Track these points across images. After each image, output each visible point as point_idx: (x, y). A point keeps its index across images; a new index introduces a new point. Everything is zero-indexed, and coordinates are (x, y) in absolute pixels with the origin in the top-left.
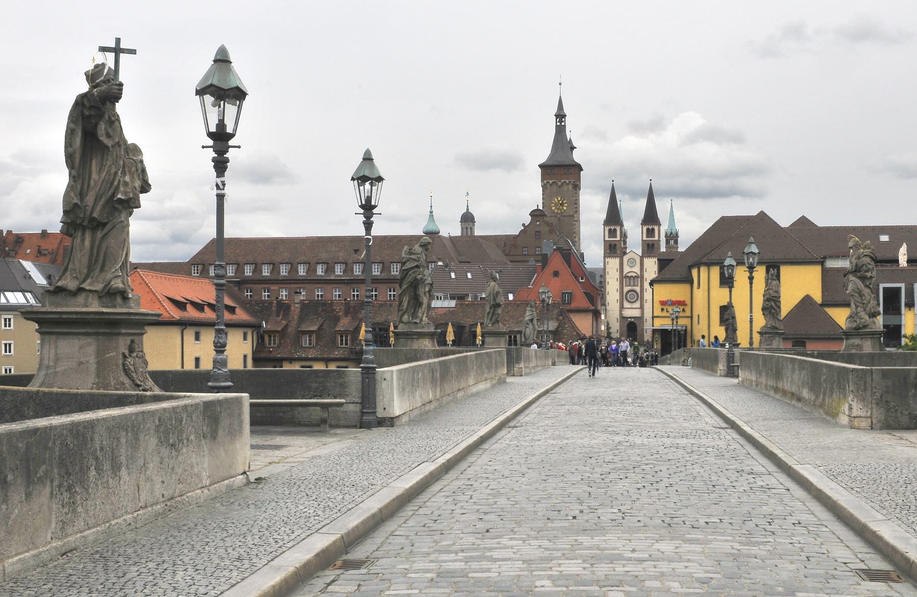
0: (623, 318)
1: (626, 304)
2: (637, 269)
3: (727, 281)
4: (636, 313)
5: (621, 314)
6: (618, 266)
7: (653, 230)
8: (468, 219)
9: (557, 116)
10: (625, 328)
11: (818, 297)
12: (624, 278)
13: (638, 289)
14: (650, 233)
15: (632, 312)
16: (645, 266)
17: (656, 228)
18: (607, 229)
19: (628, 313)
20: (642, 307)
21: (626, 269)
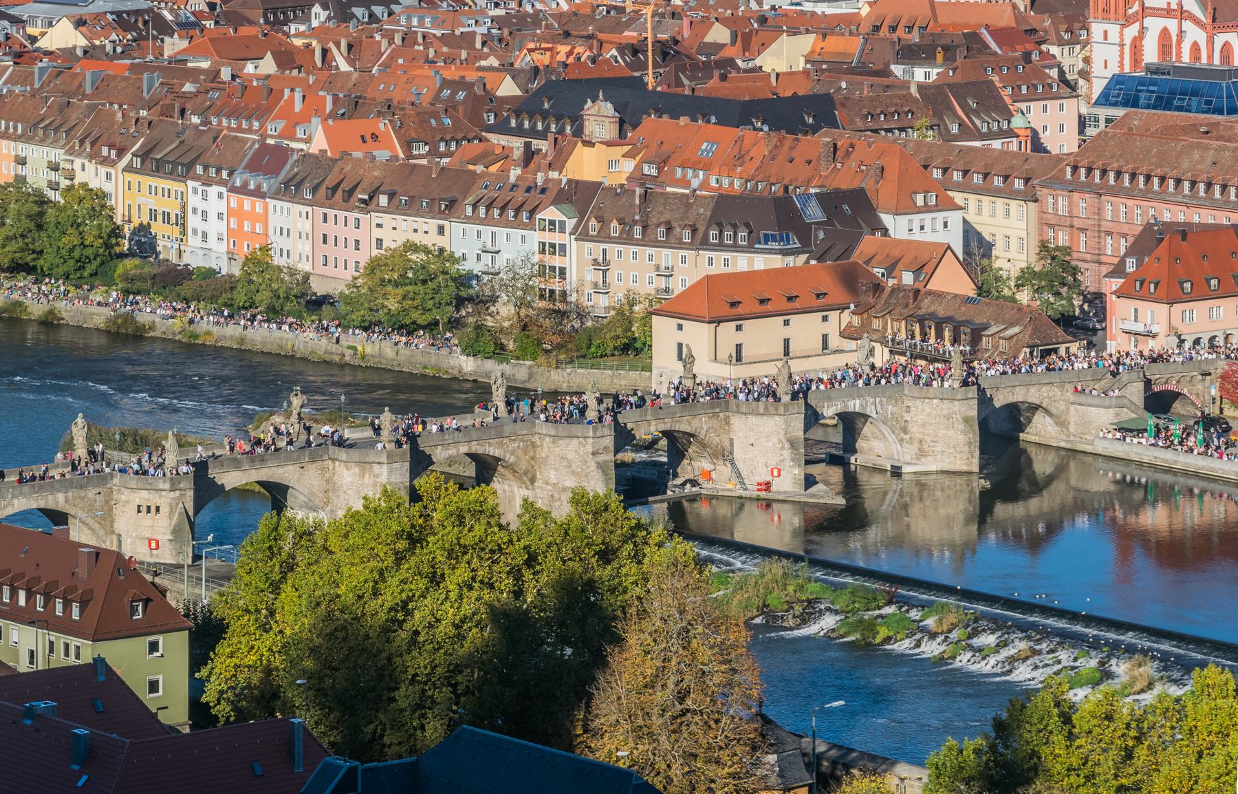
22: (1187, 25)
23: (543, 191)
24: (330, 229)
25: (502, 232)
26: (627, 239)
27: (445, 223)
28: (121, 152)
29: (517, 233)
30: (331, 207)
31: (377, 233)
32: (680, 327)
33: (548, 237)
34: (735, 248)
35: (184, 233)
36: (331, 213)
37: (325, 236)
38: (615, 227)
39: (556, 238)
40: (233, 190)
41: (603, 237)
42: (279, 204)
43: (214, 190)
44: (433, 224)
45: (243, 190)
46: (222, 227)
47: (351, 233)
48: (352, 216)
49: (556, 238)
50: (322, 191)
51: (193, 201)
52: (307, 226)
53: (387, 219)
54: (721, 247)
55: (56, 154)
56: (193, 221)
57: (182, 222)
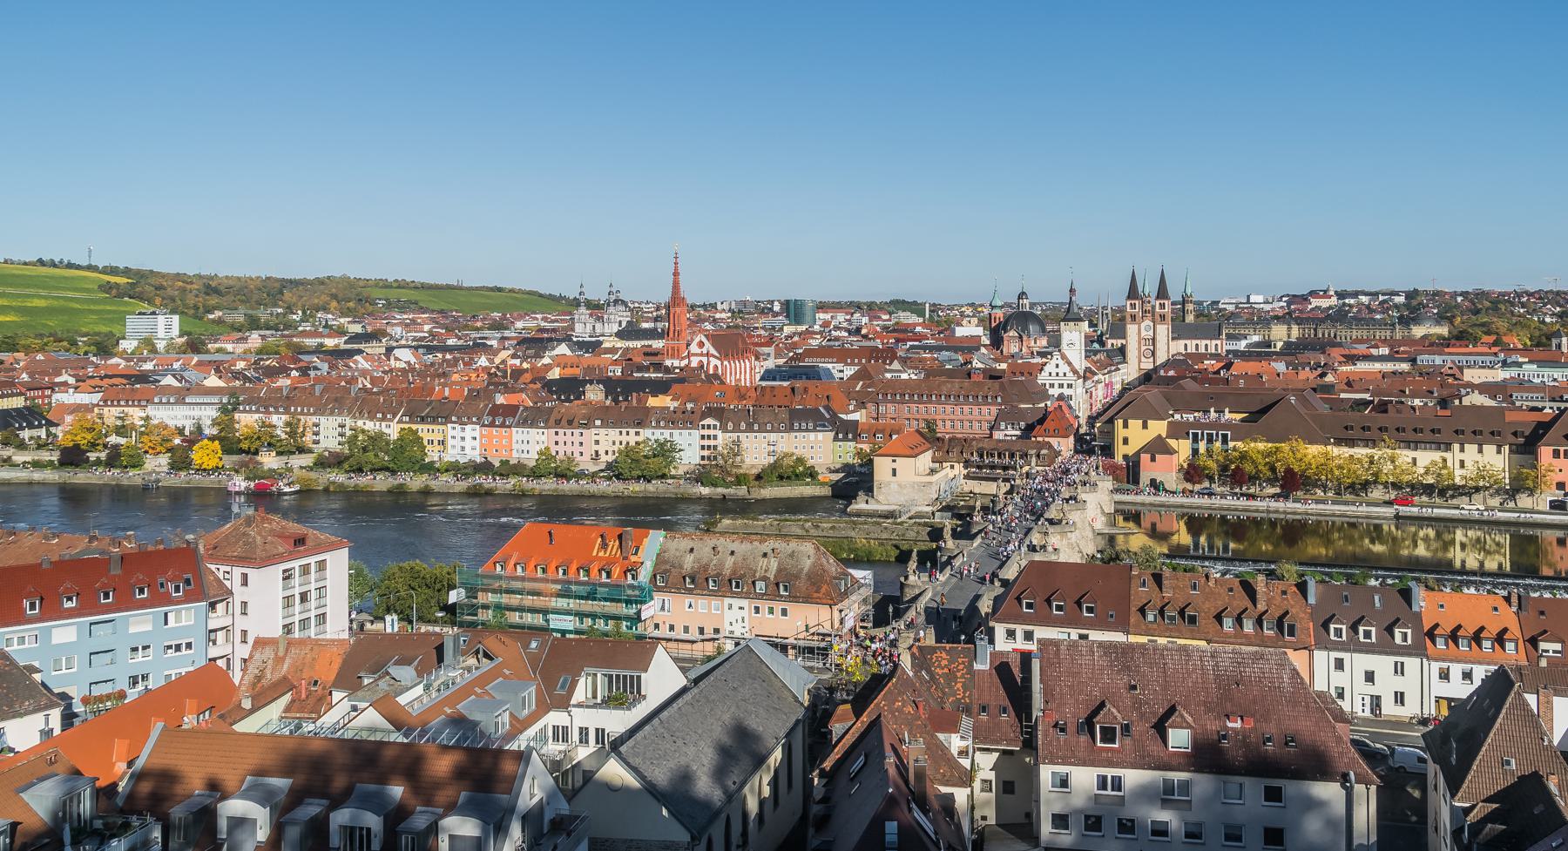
1: (1143, 359)
2: (1151, 333)
3: (1126, 426)
9: (1071, 291)
14: (1162, 306)
16: (1158, 331)
18: (1129, 303)
21: (1144, 333)
22: (711, 359)
23: (693, 413)
24: (561, 438)
25: (676, 432)
26: (750, 429)
27: (641, 430)
28: (394, 417)
30: (561, 428)
32: (894, 461)
33: (706, 432)
34: (807, 430)
36: (561, 431)
38: (743, 426)
39: (712, 432)
40: (484, 425)
41: (736, 429)
42: (520, 430)
43: (468, 428)
44: (632, 431)
45: (492, 425)
46: (477, 443)
48: (577, 432)
49: (712, 432)
50: (552, 421)
51: (451, 433)
53: (603, 431)
54: (800, 430)
55: (339, 420)
56: (450, 442)
57: (442, 443)
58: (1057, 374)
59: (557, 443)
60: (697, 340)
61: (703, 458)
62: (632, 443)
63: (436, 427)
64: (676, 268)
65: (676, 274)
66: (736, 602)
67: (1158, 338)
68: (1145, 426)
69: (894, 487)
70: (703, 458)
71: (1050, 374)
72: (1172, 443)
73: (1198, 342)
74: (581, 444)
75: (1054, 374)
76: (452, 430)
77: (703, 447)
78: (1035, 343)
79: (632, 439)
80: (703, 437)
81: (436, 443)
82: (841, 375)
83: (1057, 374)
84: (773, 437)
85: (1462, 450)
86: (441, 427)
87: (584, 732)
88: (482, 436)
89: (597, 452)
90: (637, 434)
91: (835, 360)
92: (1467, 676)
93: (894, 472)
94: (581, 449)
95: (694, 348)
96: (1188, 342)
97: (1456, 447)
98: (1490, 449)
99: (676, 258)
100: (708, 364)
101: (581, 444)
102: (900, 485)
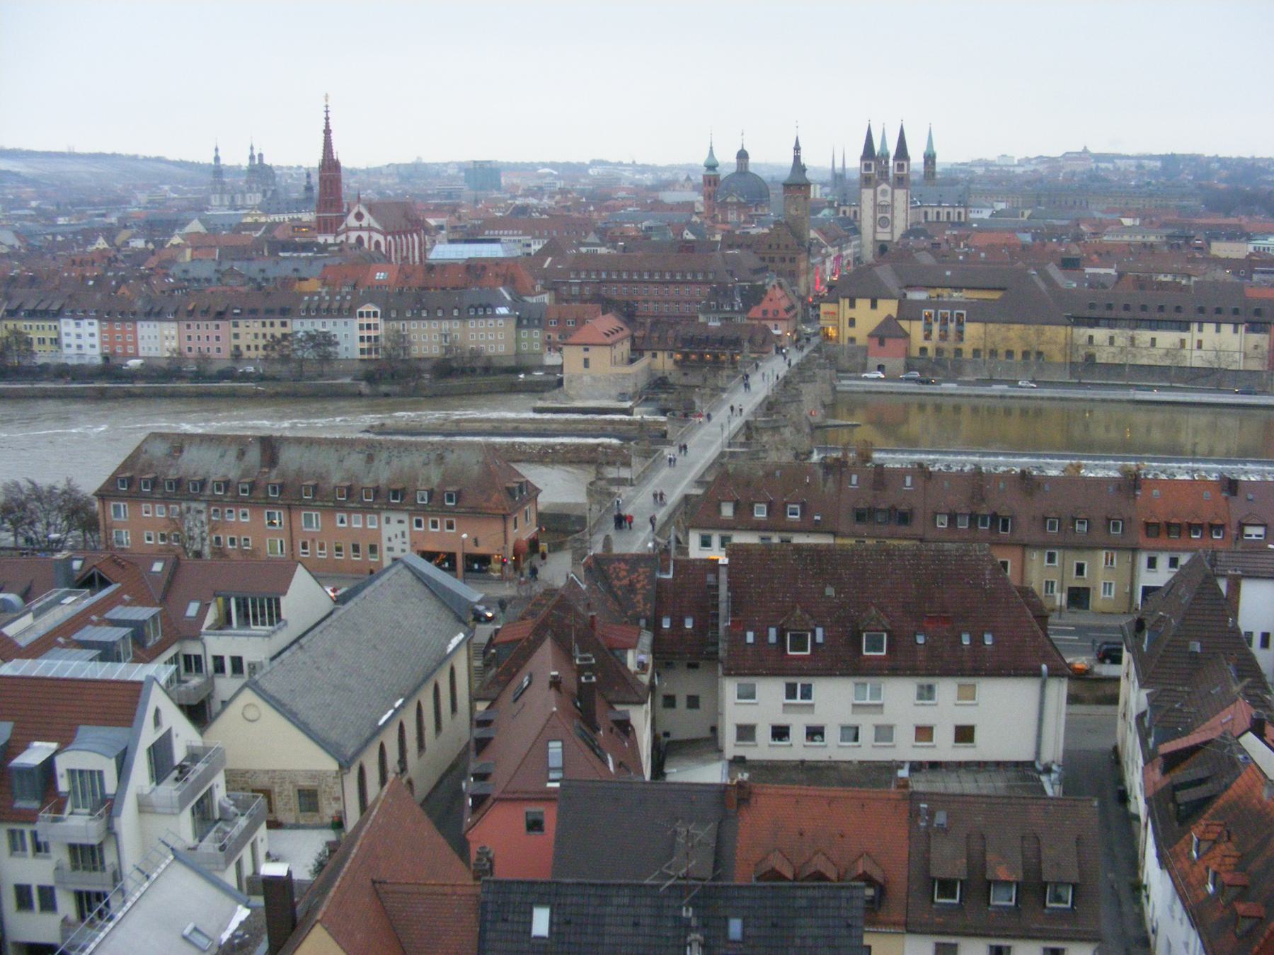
0: (875, 241)
1: (879, 229)
2: (888, 199)
3: (852, 305)
4: (887, 237)
5: (874, 237)
6: (872, 196)
7: (903, 165)
8: (743, 155)
10: (877, 250)
11: (894, 315)
12: (877, 206)
13: (889, 216)
15: (884, 235)
16: (896, 196)
17: (905, 164)
19: (880, 237)
20: (892, 232)
21: (880, 198)
24: (191, 332)
26: (417, 317)
27: (288, 321)
29: (340, 322)
31: (235, 330)
32: (586, 350)
33: (365, 321)
34: (485, 316)
35: (60, 347)
36: (194, 324)
37: (199, 337)
39: (372, 321)
43: (85, 322)
44: (277, 322)
47: (213, 332)
49: (372, 321)
52: (174, 332)
54: (476, 316)
56: (65, 340)
57: (56, 342)
58: (778, 246)
59: (189, 337)
60: (355, 211)
61: (362, 351)
62: (278, 335)
63: (47, 324)
64: (327, 125)
65: (327, 132)
66: (394, 517)
67: (896, 204)
68: (874, 306)
69: (587, 379)
70: (362, 351)
71: (770, 246)
72: (905, 324)
73: (940, 210)
74: (218, 338)
75: (774, 246)
76: (67, 326)
77: (362, 339)
78: (756, 210)
79: (278, 331)
80: (361, 327)
81: (48, 342)
82: (527, 250)
83: (778, 246)
84: (446, 325)
85: (1200, 330)
86: (53, 324)
87: (219, 660)
88: (102, 332)
89: (237, 348)
90: (284, 324)
91: (520, 232)
92: (1173, 563)
93: (586, 363)
94: (218, 344)
95: (351, 221)
96: (929, 210)
97: (1195, 327)
98: (1227, 329)
99: (327, 112)
100: (370, 238)
101: (218, 338)
102: (594, 379)
